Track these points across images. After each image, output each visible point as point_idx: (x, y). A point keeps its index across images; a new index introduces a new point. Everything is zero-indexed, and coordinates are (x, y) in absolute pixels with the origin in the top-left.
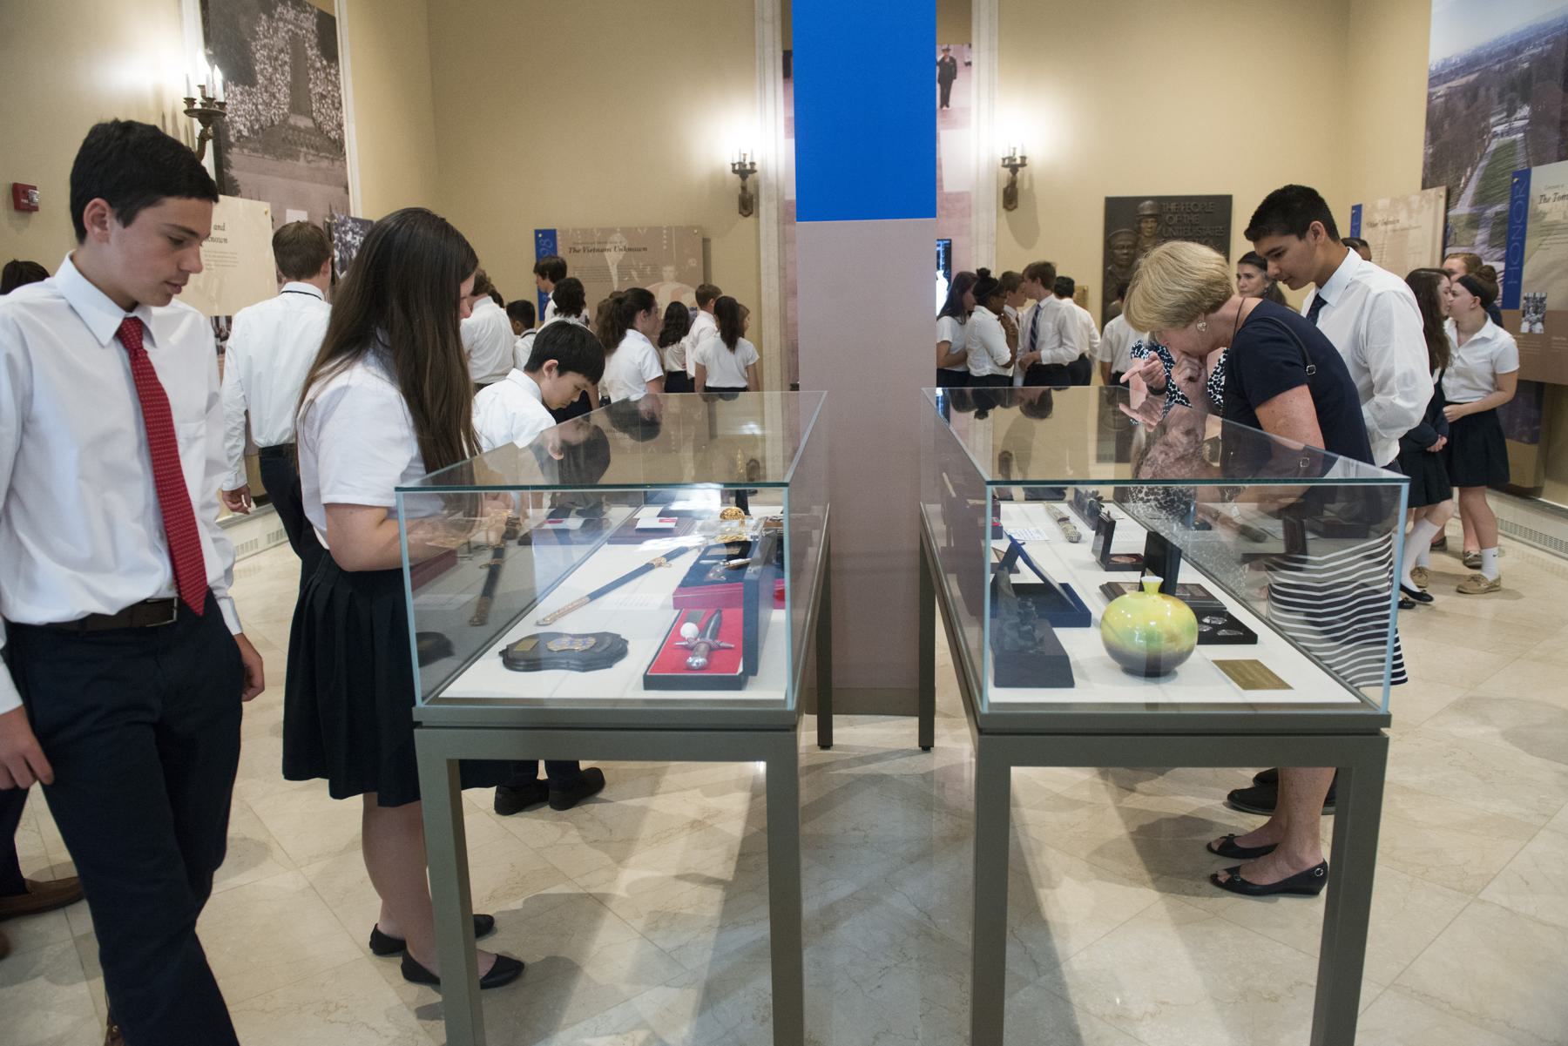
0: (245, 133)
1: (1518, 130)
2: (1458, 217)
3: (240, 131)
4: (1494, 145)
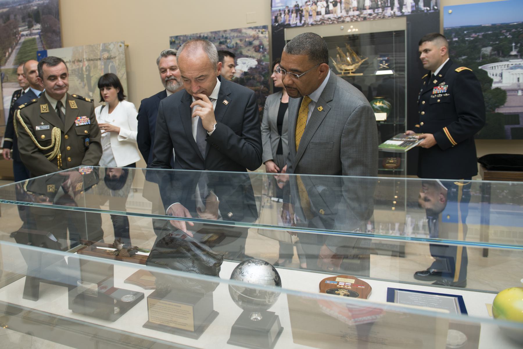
1: (35, 34)
2: (7, 70)
4: (23, 39)
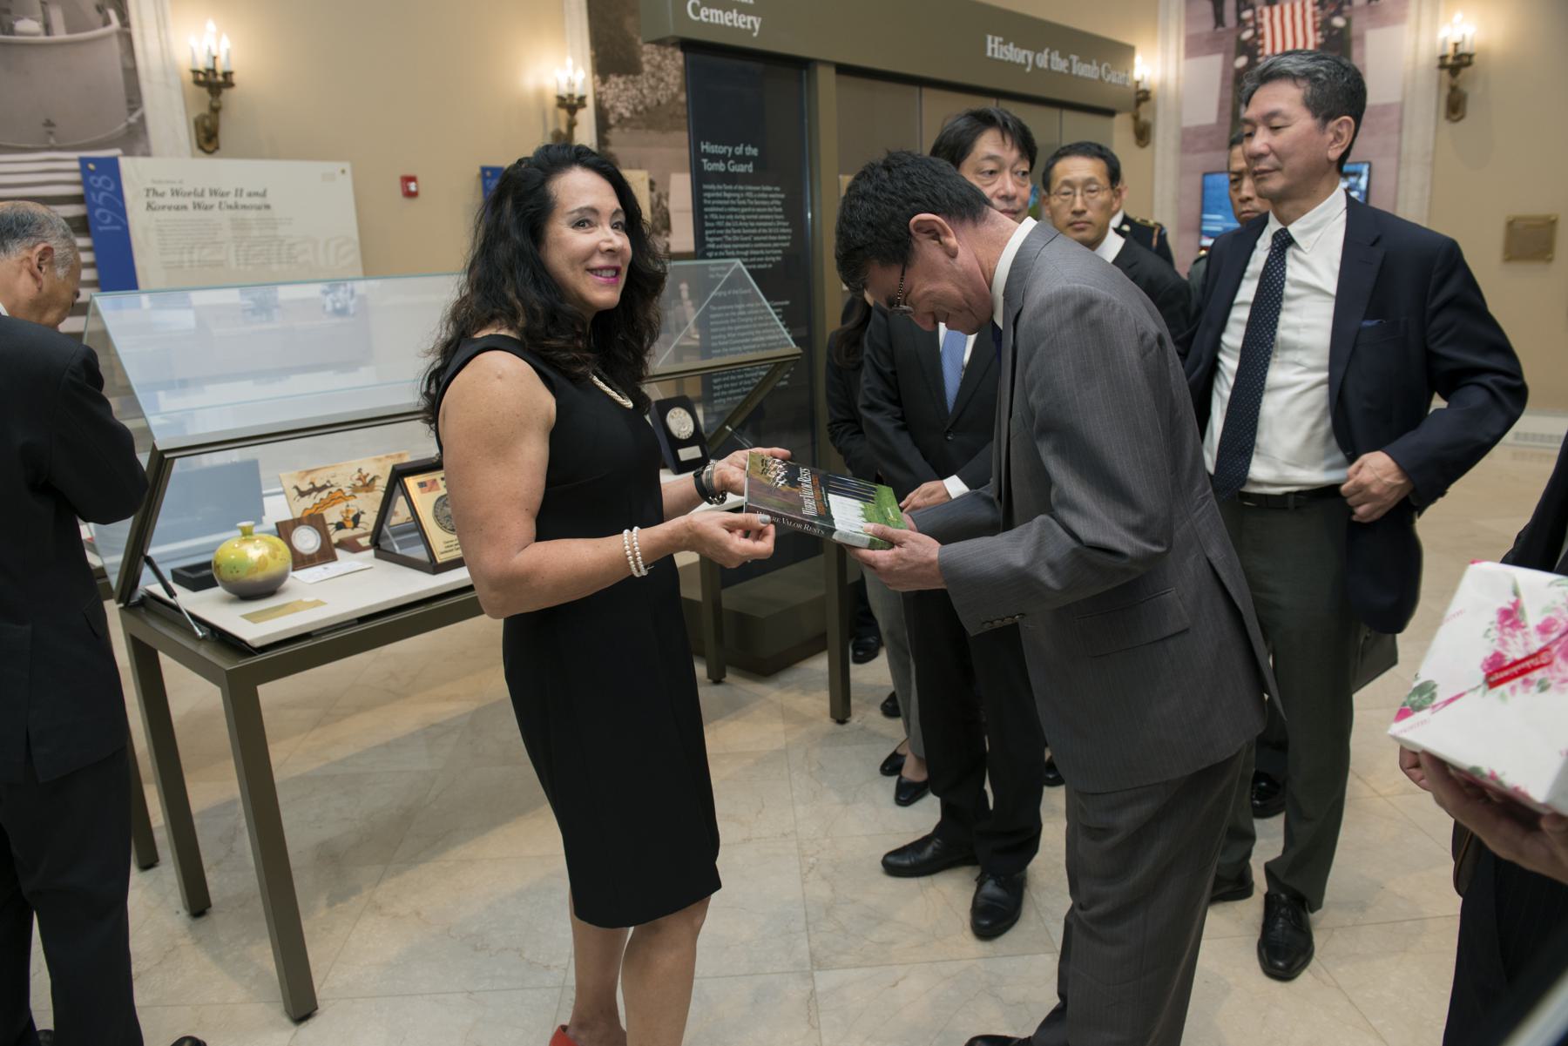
0: (627, 114)
3: (621, 115)
